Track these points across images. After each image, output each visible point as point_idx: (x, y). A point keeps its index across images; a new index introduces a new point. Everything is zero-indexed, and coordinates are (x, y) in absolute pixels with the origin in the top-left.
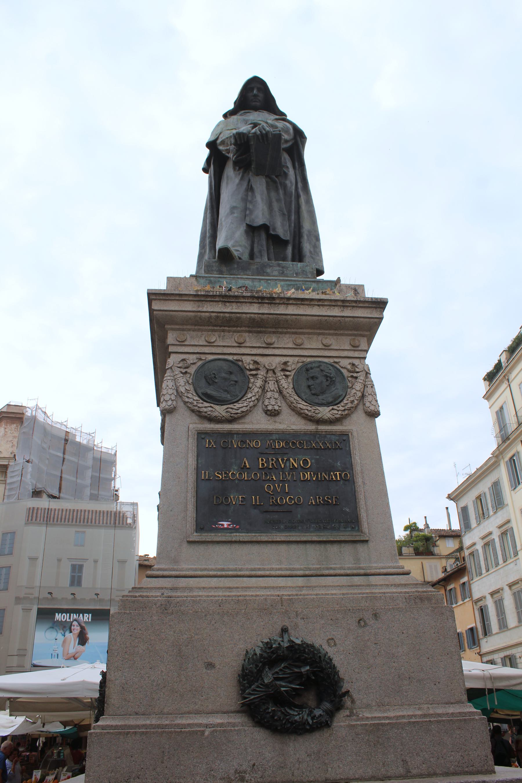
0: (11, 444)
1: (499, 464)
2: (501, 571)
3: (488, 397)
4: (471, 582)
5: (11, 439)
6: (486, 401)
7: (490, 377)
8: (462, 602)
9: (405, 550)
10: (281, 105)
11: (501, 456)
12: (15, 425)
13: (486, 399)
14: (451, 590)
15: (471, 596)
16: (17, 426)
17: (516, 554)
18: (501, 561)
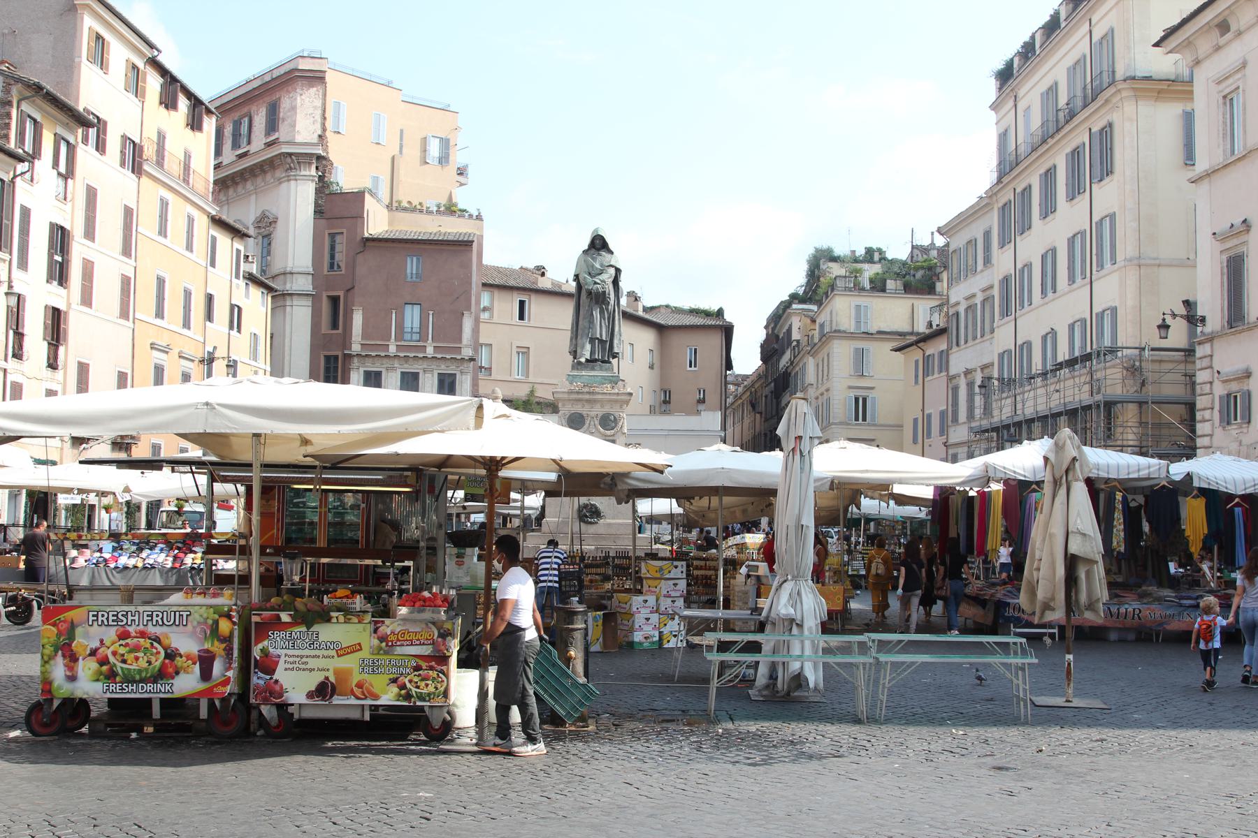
0: (312, 119)
1: (993, 208)
2: (978, 347)
3: (995, 107)
4: (950, 352)
5: (311, 111)
6: (993, 112)
7: (1005, 75)
8: (938, 376)
9: (890, 284)
10: (611, 246)
11: (995, 198)
12: (315, 89)
13: (993, 110)
14: (929, 355)
15: (947, 370)
16: (317, 91)
17: (992, 331)
18: (979, 336)
